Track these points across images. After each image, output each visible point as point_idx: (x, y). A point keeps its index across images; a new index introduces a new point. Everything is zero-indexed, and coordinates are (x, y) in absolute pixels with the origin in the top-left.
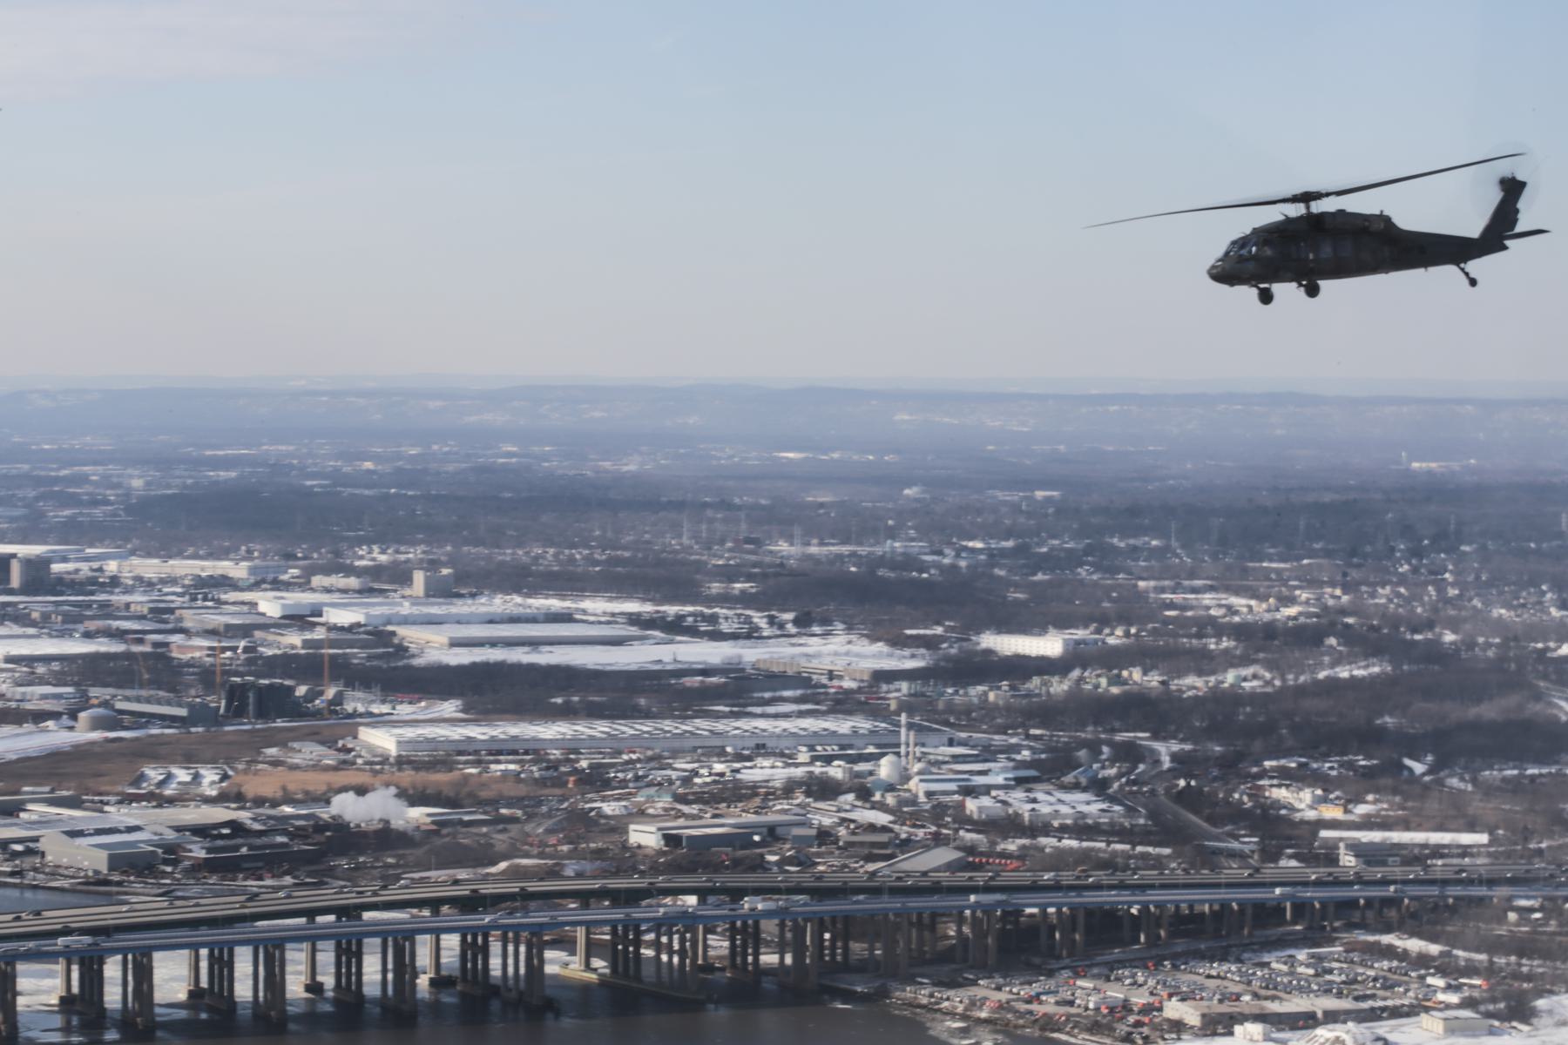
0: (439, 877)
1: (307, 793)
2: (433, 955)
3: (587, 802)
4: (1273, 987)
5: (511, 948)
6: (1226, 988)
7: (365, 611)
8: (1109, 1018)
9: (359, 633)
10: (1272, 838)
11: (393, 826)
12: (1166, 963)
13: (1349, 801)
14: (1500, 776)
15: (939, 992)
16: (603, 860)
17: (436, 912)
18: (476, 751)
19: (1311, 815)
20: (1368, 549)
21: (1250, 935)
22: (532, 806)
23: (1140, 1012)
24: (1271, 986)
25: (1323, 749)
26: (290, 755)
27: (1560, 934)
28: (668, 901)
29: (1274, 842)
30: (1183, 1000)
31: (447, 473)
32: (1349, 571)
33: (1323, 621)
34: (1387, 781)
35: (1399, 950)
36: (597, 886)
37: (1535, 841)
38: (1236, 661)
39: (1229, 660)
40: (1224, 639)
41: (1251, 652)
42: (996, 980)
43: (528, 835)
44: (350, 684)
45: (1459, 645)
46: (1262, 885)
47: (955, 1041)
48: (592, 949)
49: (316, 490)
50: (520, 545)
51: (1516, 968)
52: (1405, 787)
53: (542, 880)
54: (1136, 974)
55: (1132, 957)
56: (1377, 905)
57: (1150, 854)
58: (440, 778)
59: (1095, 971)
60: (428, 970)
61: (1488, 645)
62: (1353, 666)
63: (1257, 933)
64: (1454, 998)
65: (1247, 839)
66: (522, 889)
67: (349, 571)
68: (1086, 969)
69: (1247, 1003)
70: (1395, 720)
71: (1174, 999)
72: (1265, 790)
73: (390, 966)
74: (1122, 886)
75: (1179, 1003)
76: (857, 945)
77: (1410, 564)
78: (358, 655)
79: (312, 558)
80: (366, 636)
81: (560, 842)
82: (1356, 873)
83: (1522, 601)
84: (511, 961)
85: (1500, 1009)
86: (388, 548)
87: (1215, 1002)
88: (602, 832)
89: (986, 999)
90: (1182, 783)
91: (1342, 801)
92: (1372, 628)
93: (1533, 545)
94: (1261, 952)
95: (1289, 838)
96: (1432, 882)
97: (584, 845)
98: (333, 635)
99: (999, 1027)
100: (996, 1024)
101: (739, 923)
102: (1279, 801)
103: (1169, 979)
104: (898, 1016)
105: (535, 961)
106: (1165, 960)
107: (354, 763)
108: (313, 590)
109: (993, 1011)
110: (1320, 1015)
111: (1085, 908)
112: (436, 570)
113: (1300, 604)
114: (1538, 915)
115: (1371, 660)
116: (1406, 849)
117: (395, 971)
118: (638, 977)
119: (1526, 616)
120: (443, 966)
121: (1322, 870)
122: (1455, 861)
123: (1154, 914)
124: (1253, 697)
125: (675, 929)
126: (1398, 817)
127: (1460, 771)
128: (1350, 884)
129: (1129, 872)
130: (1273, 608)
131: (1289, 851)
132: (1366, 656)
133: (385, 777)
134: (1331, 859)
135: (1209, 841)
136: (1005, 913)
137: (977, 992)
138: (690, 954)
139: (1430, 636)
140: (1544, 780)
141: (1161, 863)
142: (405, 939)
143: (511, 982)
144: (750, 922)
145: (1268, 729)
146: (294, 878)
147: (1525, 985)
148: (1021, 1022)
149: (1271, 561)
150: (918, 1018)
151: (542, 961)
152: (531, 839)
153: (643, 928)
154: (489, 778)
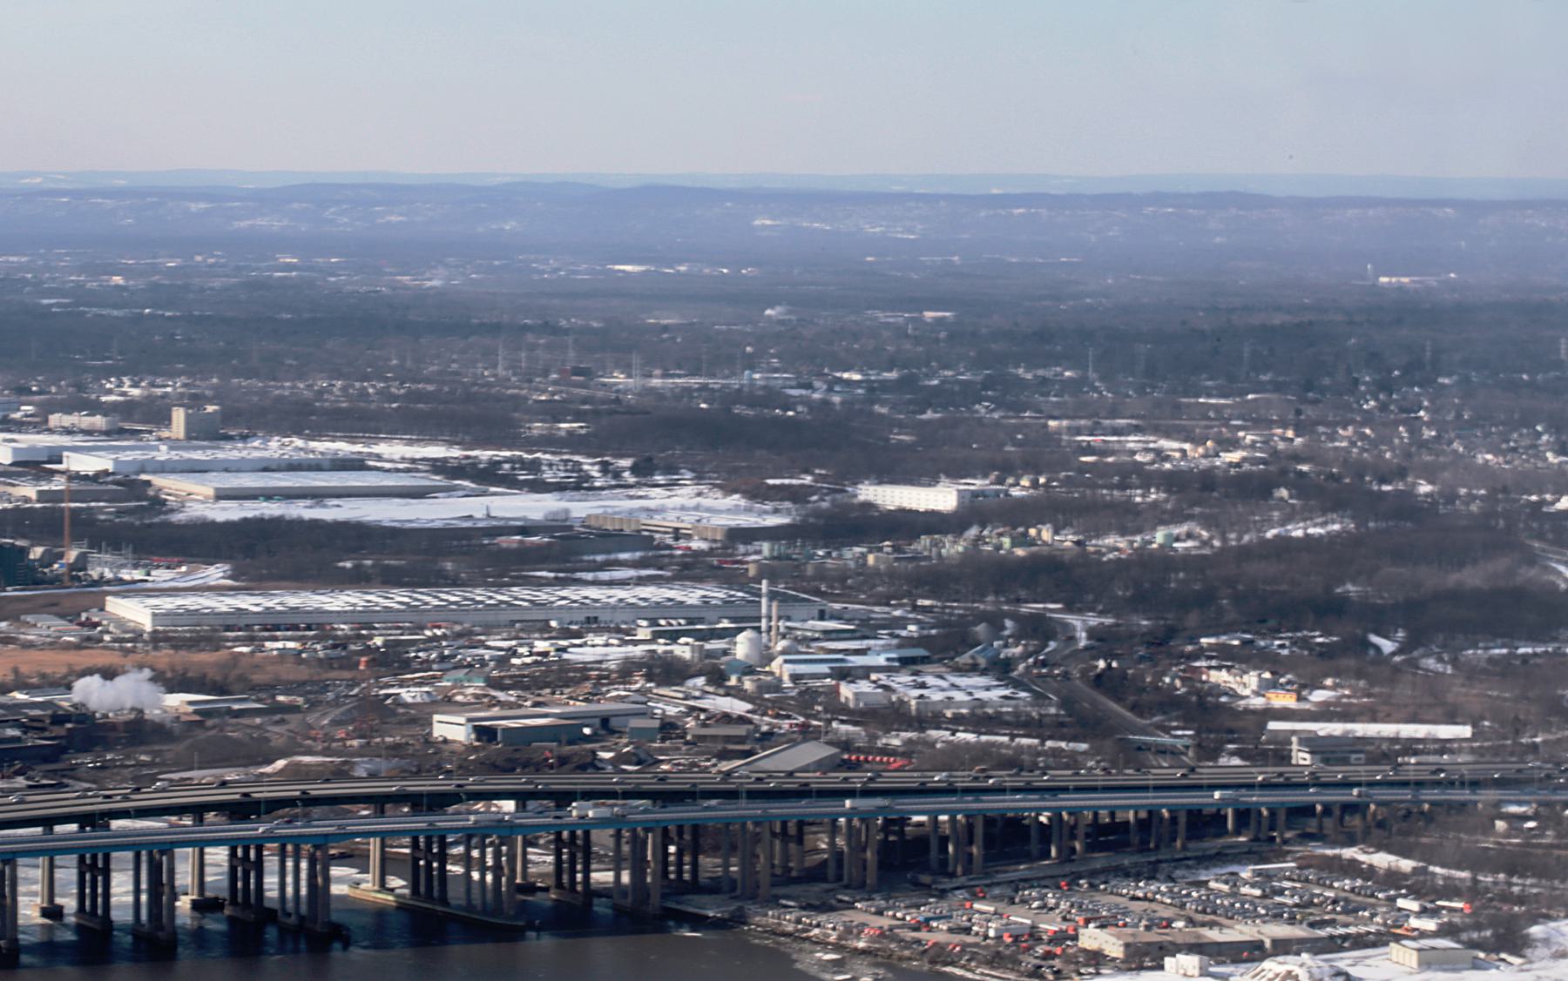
0: (204, 778)
1: (43, 676)
2: (196, 872)
3: (382, 688)
4: (1211, 912)
5: (290, 864)
6: (1154, 912)
7: (114, 456)
8: (1014, 948)
9: (107, 483)
10: (1210, 731)
11: (146, 717)
12: (1081, 882)
13: (1303, 686)
14: (1486, 656)
15: (808, 917)
16: (402, 757)
17: (200, 820)
18: (247, 626)
19: (1257, 702)
20: (1327, 381)
21: (1184, 848)
22: (316, 693)
23: (1050, 942)
24: (1208, 910)
25: (1272, 623)
26: (22, 630)
27: (1558, 847)
28: (480, 806)
29: (1212, 736)
30: (1102, 927)
31: (212, 289)
32: (1302, 407)
33: (1272, 468)
34: (1350, 662)
35: (1364, 866)
36: (394, 789)
37: (1528, 735)
38: (1166, 517)
39: (1161, 516)
40: (1153, 490)
41: (1185, 506)
42: (876, 903)
43: (310, 727)
44: (95, 545)
45: (1436, 496)
46: (1199, 787)
47: (827, 976)
48: (388, 865)
49: (54, 310)
50: (301, 376)
51: (1505, 887)
52: (1371, 669)
53: (327, 781)
54: (1046, 895)
55: (1041, 875)
56: (1337, 812)
57: (1063, 750)
58: (204, 658)
59: (997, 891)
60: (190, 892)
61: (1472, 498)
62: (1308, 522)
63: (1191, 845)
64: (1430, 925)
65: (1180, 733)
66: (304, 792)
67: (95, 408)
68: (986, 889)
69: (1180, 930)
70: (1359, 589)
71: (1091, 925)
72: (1202, 673)
73: (144, 886)
74: (1029, 789)
75: (1098, 930)
76: (708, 860)
77: (1377, 400)
78: (105, 509)
79: (49, 392)
80: (114, 487)
81: (350, 736)
82: (1312, 773)
83: (1512, 444)
84: (289, 879)
85: (1485, 938)
86: (142, 380)
87: (1142, 929)
88: (400, 723)
89: (864, 925)
90: (1102, 664)
91: (1295, 687)
92: (1331, 476)
93: (1525, 377)
94: (1197, 869)
95: (1231, 731)
96: (1405, 784)
97: (378, 740)
98: (75, 486)
99: (880, 960)
100: (877, 955)
101: (565, 834)
102: (1219, 685)
103: (1085, 902)
104: (758, 946)
105: (320, 880)
106: (1081, 878)
107: (101, 640)
108: (51, 431)
109: (872, 940)
110: (1268, 944)
111: (985, 816)
112: (200, 407)
113: (1244, 448)
114: (1531, 824)
115: (1330, 516)
116: (1373, 744)
117: (151, 892)
118: (444, 900)
119: (1516, 463)
120: (207, 886)
121: (1269, 769)
122: (1432, 759)
123: (1068, 822)
124: (1187, 560)
125: (488, 841)
126: (1364, 705)
127: (1437, 650)
128: (1305, 786)
129: (1037, 772)
130: (1211, 452)
131: (1230, 746)
132: (1324, 512)
133: (138, 657)
134: (1284, 757)
135: (1135, 735)
136: (887, 822)
137: (854, 917)
138: (506, 871)
139: (1401, 486)
140: (1539, 661)
141: (1076, 761)
142: (162, 853)
143: (290, 906)
144: (579, 832)
145: (1205, 599)
146: (28, 779)
147: (1516, 909)
148: (907, 953)
149: (1209, 396)
150: (782, 948)
151: (327, 880)
152: (313, 733)
153: (450, 840)
154: (264, 658)
